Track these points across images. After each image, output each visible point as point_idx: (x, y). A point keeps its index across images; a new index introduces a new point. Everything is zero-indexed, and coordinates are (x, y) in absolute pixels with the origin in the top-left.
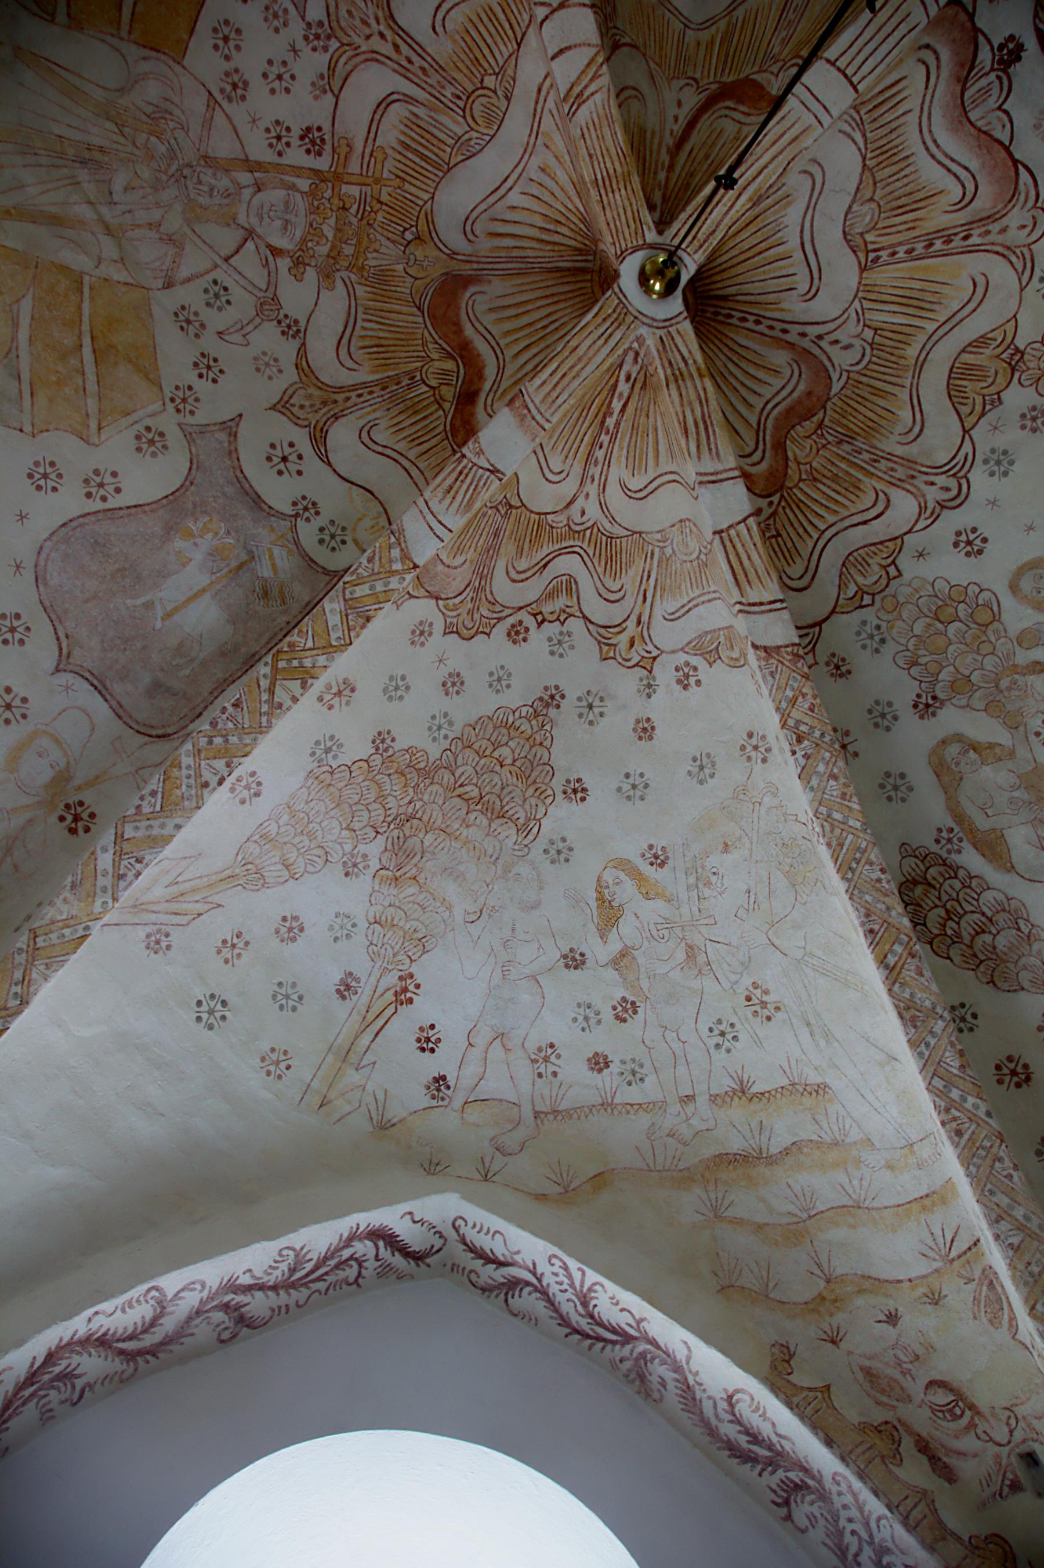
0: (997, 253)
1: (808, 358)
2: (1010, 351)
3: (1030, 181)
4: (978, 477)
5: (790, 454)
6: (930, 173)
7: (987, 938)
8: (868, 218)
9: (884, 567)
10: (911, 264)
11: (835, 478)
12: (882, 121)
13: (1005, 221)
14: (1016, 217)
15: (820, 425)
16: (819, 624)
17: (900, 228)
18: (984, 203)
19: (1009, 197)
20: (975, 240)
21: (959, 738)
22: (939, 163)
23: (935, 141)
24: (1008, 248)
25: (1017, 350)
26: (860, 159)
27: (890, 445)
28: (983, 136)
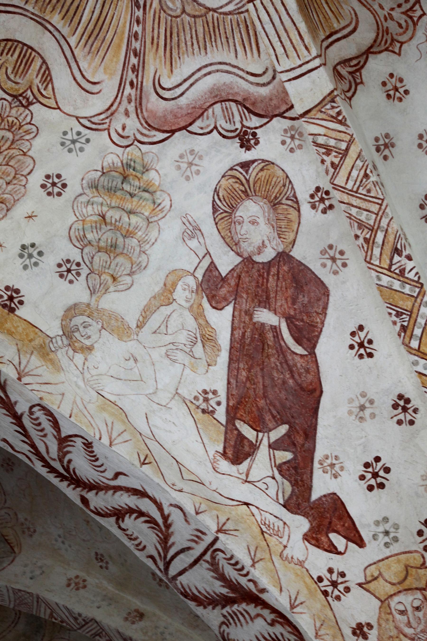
0: (112, 105)
2: (31, 98)
3: (155, 139)
6: (188, 65)
8: (170, 5)
10: (126, 35)
12: (236, 31)
13: (133, 115)
14: (133, 124)
17: (156, 31)
18: (153, 103)
19: (150, 122)
20: (128, 90)
22: (193, 74)
23: (209, 73)
24: (112, 114)
25: (31, 104)
26: (215, 7)
28: (201, 112)
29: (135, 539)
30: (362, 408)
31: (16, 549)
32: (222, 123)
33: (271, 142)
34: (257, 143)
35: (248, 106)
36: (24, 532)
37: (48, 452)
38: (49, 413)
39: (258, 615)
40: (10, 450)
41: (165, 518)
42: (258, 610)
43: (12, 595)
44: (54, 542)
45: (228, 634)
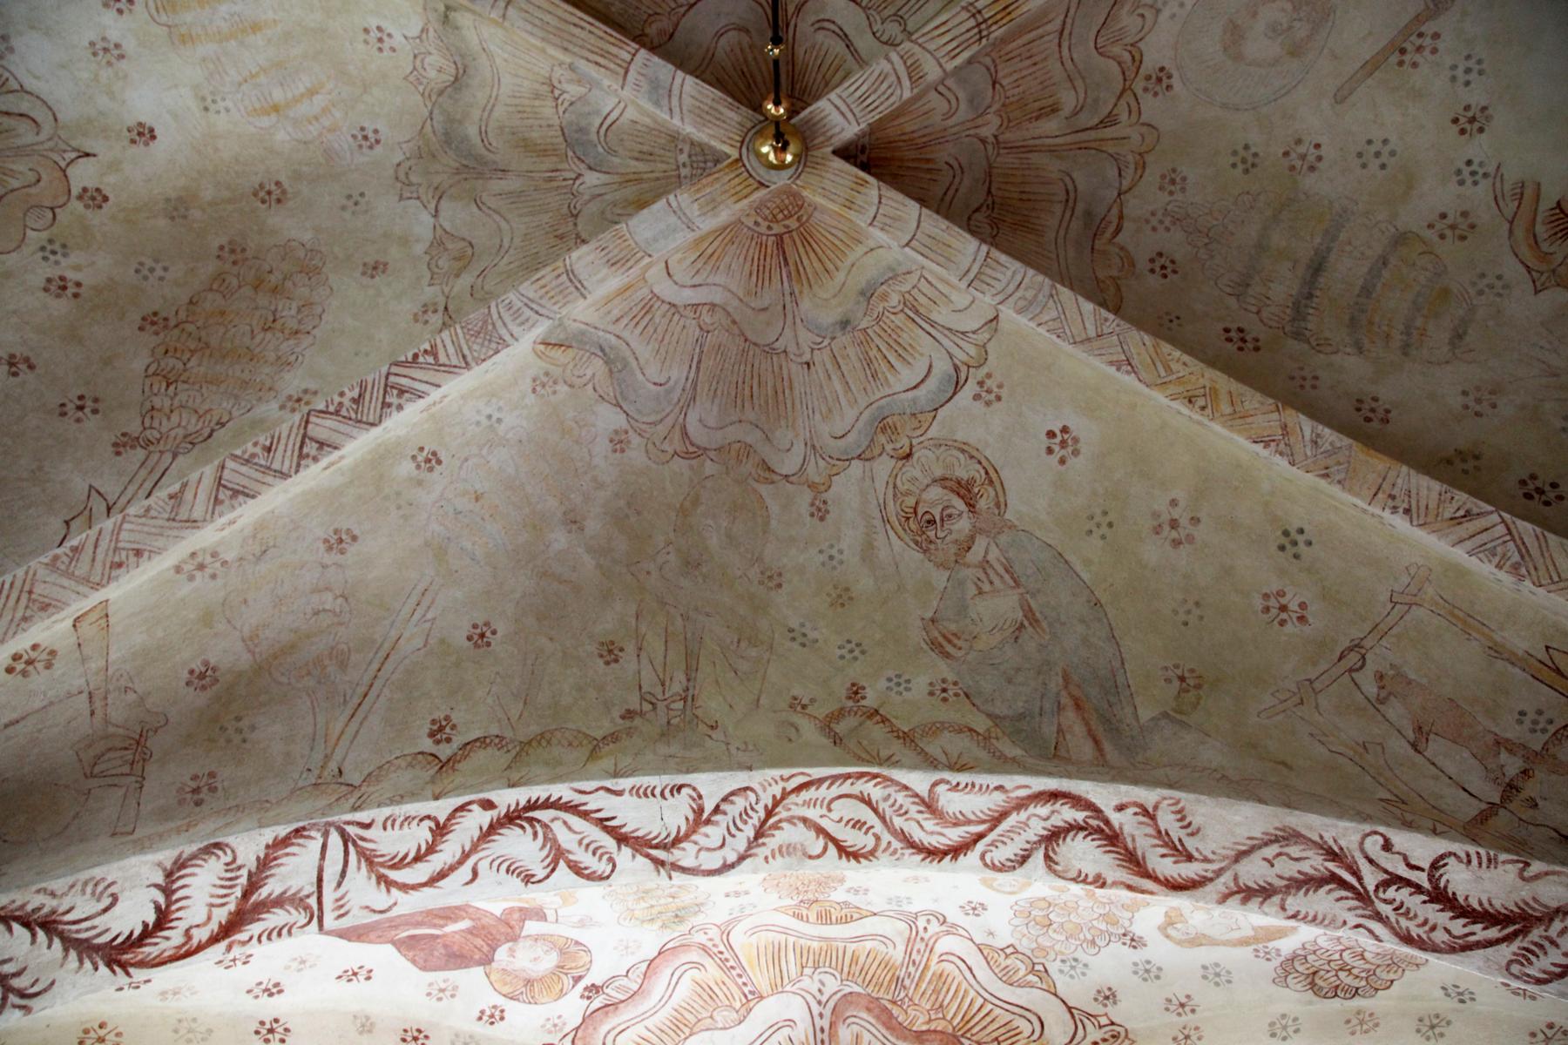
1: (840, 1010)
4: (914, 909)
5: (924, 1028)
6: (684, 990)
7: (1367, 955)
9: (1007, 956)
11: (936, 991)
13: (704, 942)
15: (894, 1003)
16: (1070, 1009)
18: (694, 956)
20: (722, 948)
21: (1163, 929)
27: (898, 954)
29: (401, 826)
30: (303, 962)
31: (542, 347)
32: (624, 982)
33: (572, 1008)
34: (582, 996)
35: (610, 1007)
36: (547, 374)
37: (565, 823)
38: (592, 877)
39: (209, 918)
40: (609, 784)
41: (390, 884)
42: (214, 926)
43: (503, 332)
44: (501, 403)
45: (218, 857)
